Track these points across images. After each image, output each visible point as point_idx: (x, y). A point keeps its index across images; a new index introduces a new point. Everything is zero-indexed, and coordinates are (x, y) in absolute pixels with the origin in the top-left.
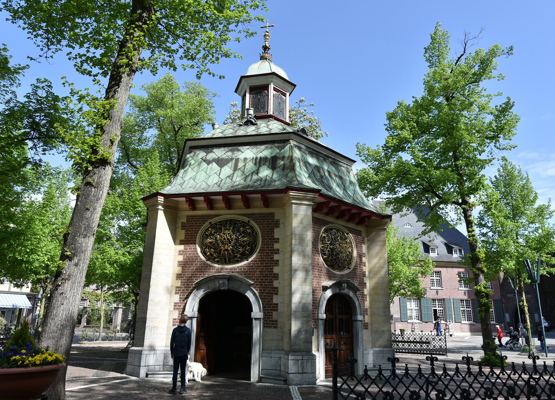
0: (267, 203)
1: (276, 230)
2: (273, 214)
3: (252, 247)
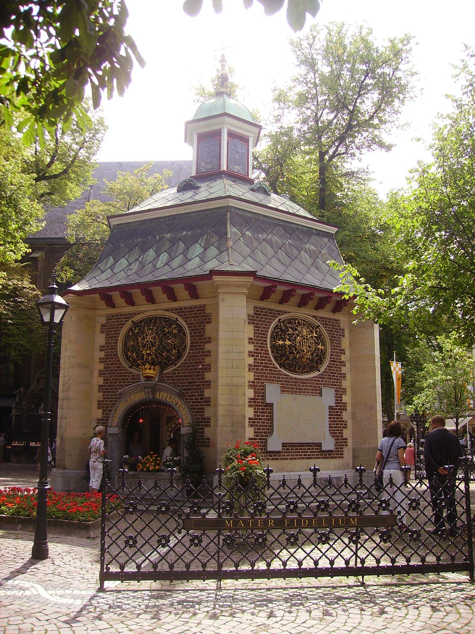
0: (194, 294)
1: (208, 326)
2: (202, 308)
3: (179, 351)
